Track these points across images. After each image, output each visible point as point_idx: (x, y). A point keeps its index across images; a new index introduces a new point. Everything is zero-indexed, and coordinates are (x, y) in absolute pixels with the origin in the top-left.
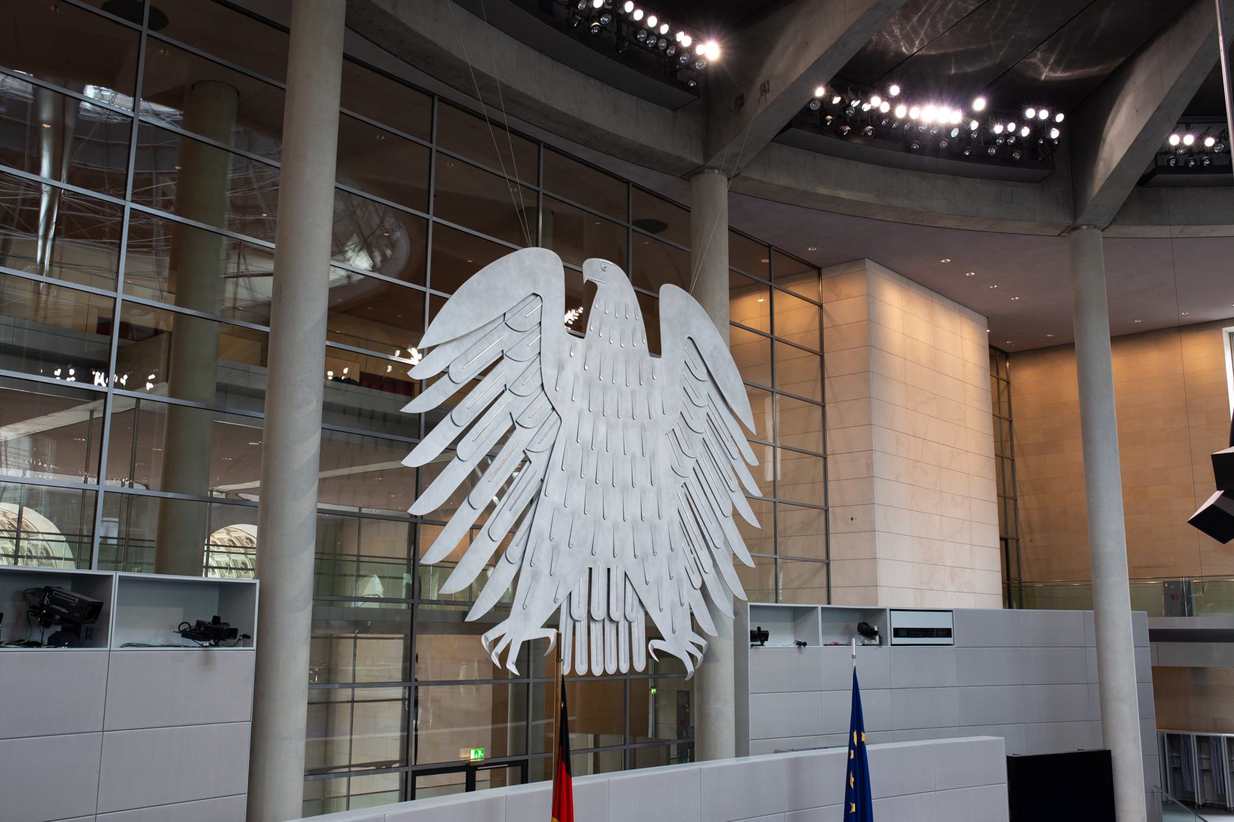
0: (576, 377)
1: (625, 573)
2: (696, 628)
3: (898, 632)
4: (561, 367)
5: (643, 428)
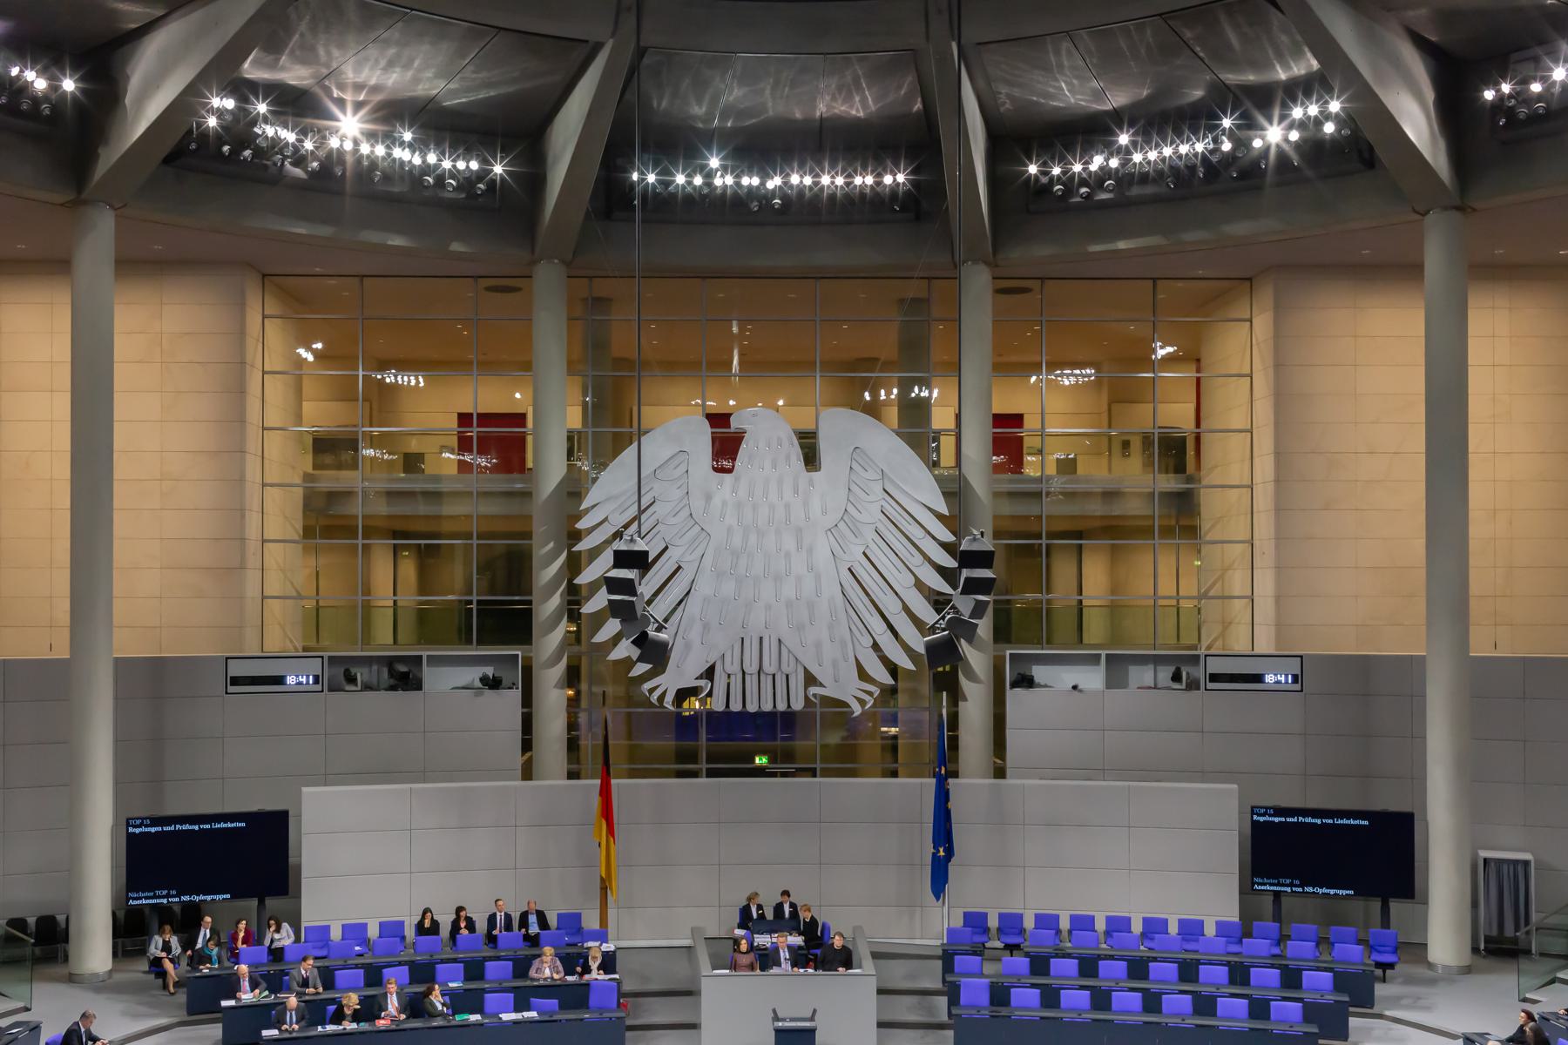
0: (724, 503)
1: (779, 640)
2: (863, 675)
3: (1215, 678)
4: (708, 498)
5: (799, 531)
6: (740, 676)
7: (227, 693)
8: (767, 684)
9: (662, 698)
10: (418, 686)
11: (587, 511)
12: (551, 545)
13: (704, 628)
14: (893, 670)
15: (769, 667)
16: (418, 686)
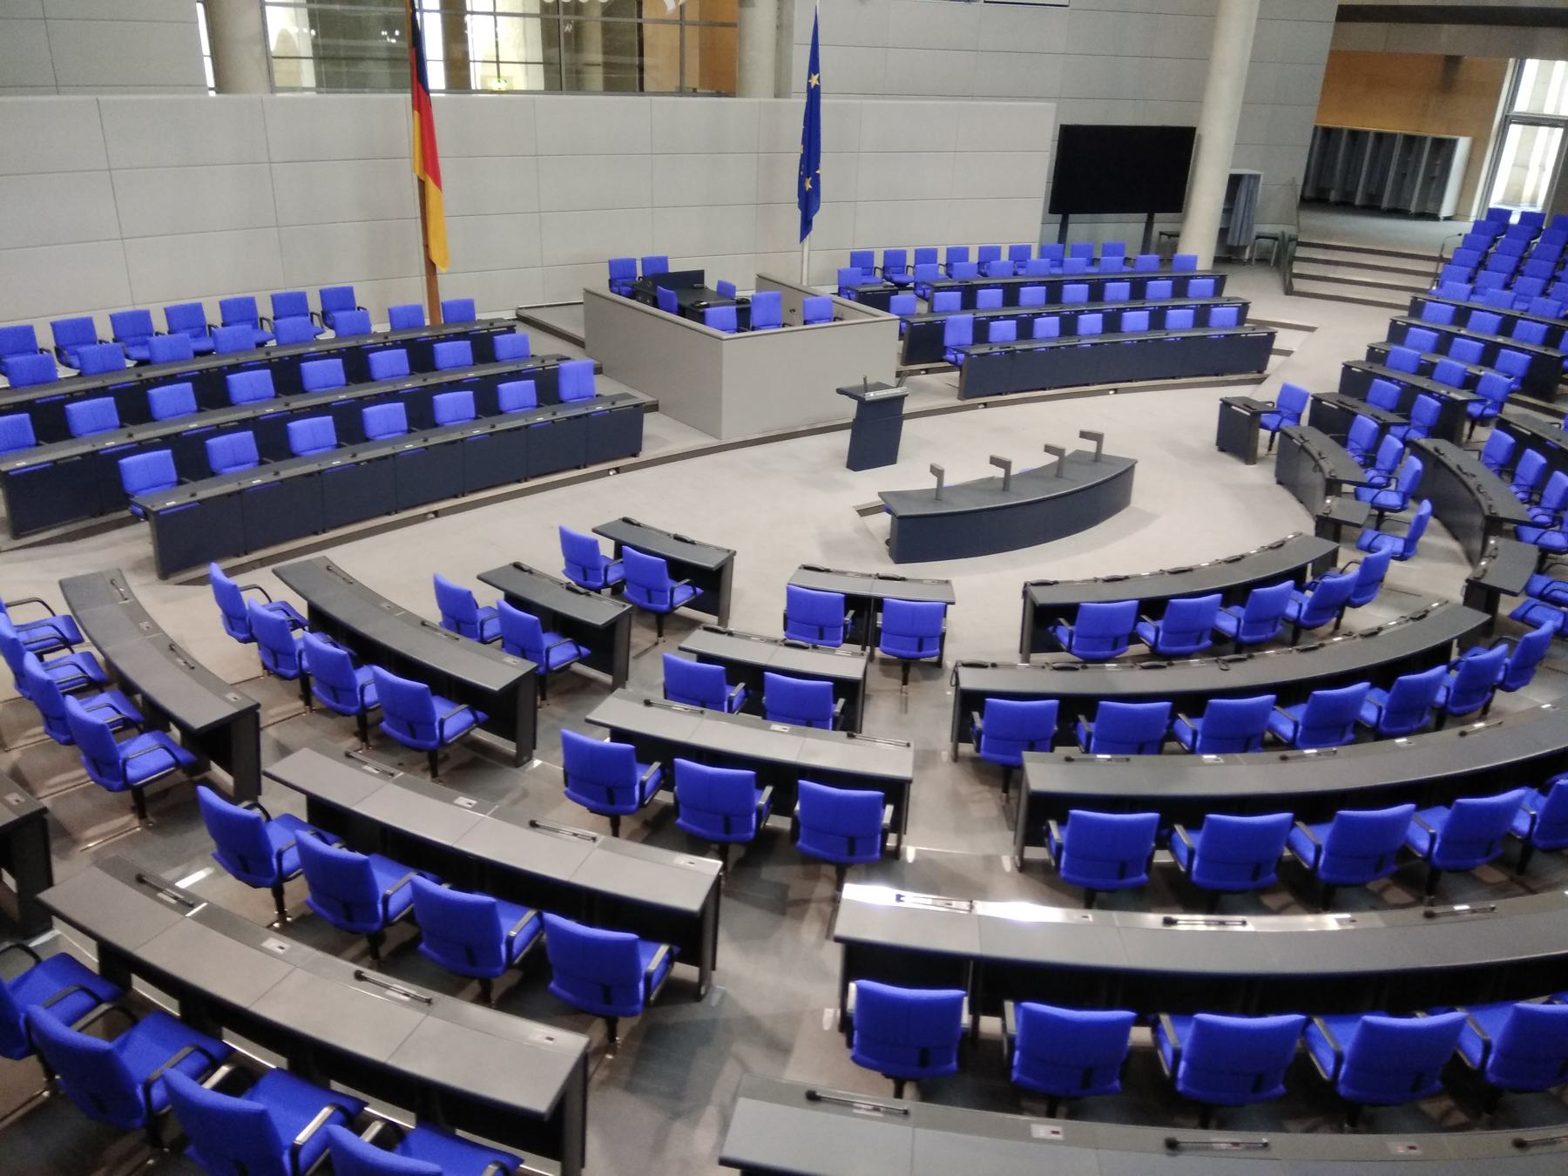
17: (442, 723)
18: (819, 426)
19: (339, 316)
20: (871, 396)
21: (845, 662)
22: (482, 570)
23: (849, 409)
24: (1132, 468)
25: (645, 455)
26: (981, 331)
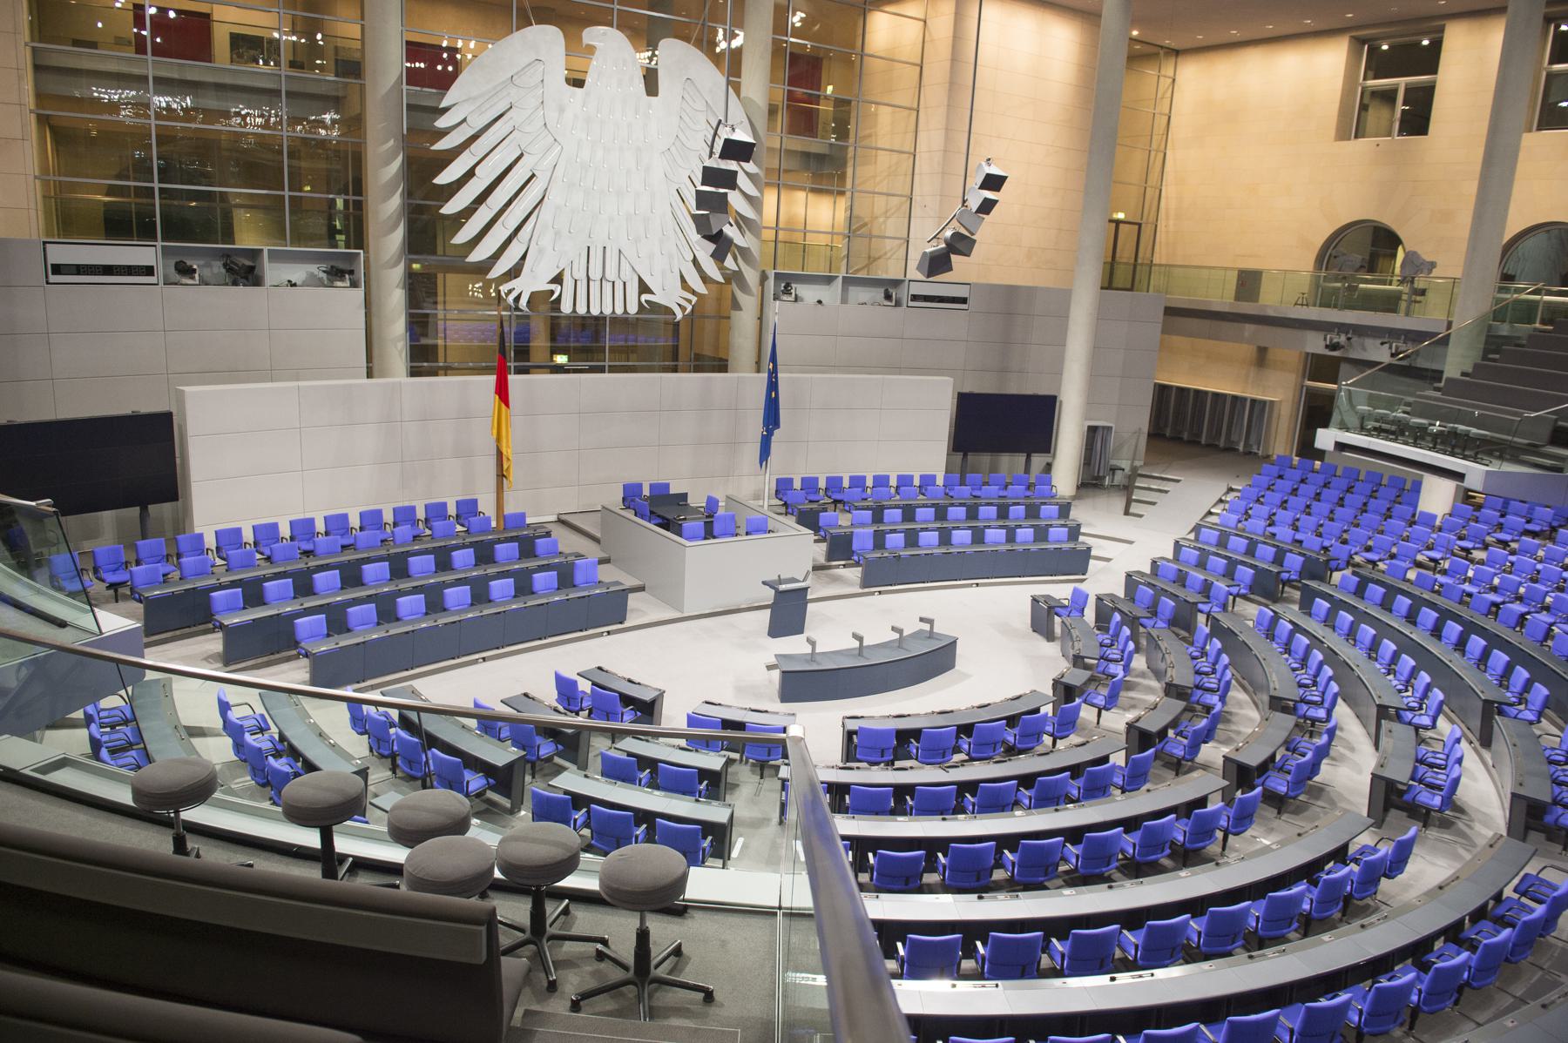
3: (915, 298)
4: (561, 110)
6: (585, 282)
7: (48, 283)
8: (608, 287)
9: (517, 299)
10: (258, 282)
11: (446, 110)
12: (392, 142)
13: (556, 234)
14: (705, 278)
15: (596, 274)
16: (258, 282)
17: (468, 782)
18: (756, 605)
19: (437, 524)
20: (783, 587)
21: (712, 761)
22: (505, 696)
23: (768, 595)
24: (955, 642)
25: (627, 624)
26: (879, 541)
